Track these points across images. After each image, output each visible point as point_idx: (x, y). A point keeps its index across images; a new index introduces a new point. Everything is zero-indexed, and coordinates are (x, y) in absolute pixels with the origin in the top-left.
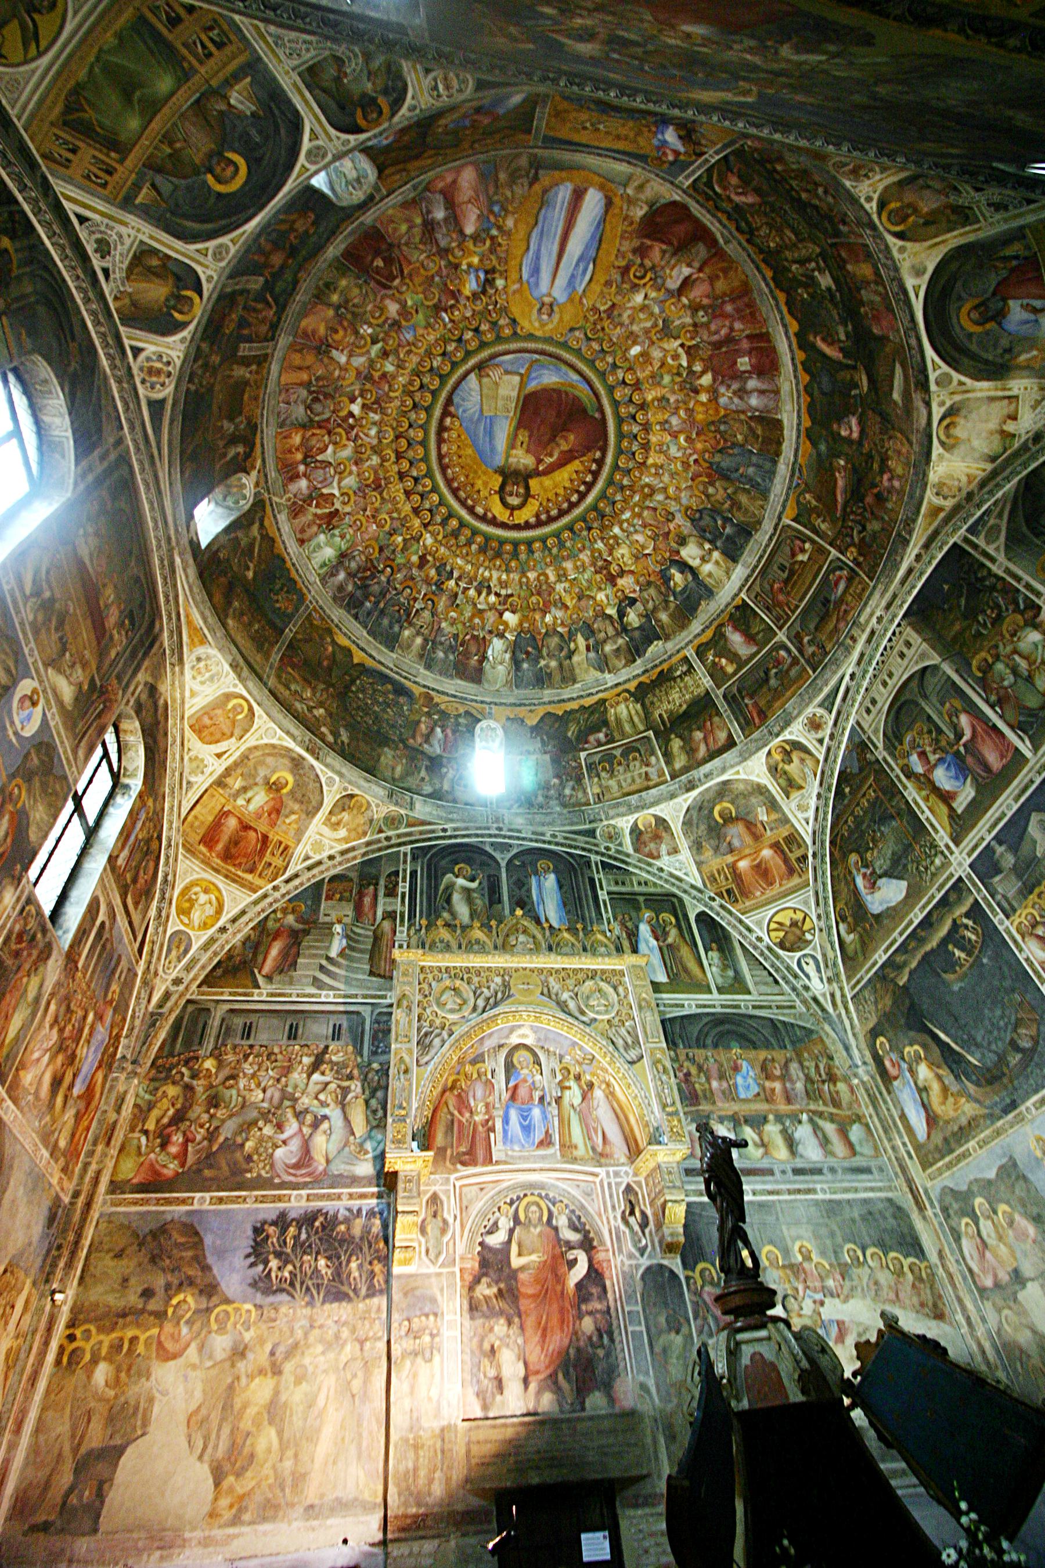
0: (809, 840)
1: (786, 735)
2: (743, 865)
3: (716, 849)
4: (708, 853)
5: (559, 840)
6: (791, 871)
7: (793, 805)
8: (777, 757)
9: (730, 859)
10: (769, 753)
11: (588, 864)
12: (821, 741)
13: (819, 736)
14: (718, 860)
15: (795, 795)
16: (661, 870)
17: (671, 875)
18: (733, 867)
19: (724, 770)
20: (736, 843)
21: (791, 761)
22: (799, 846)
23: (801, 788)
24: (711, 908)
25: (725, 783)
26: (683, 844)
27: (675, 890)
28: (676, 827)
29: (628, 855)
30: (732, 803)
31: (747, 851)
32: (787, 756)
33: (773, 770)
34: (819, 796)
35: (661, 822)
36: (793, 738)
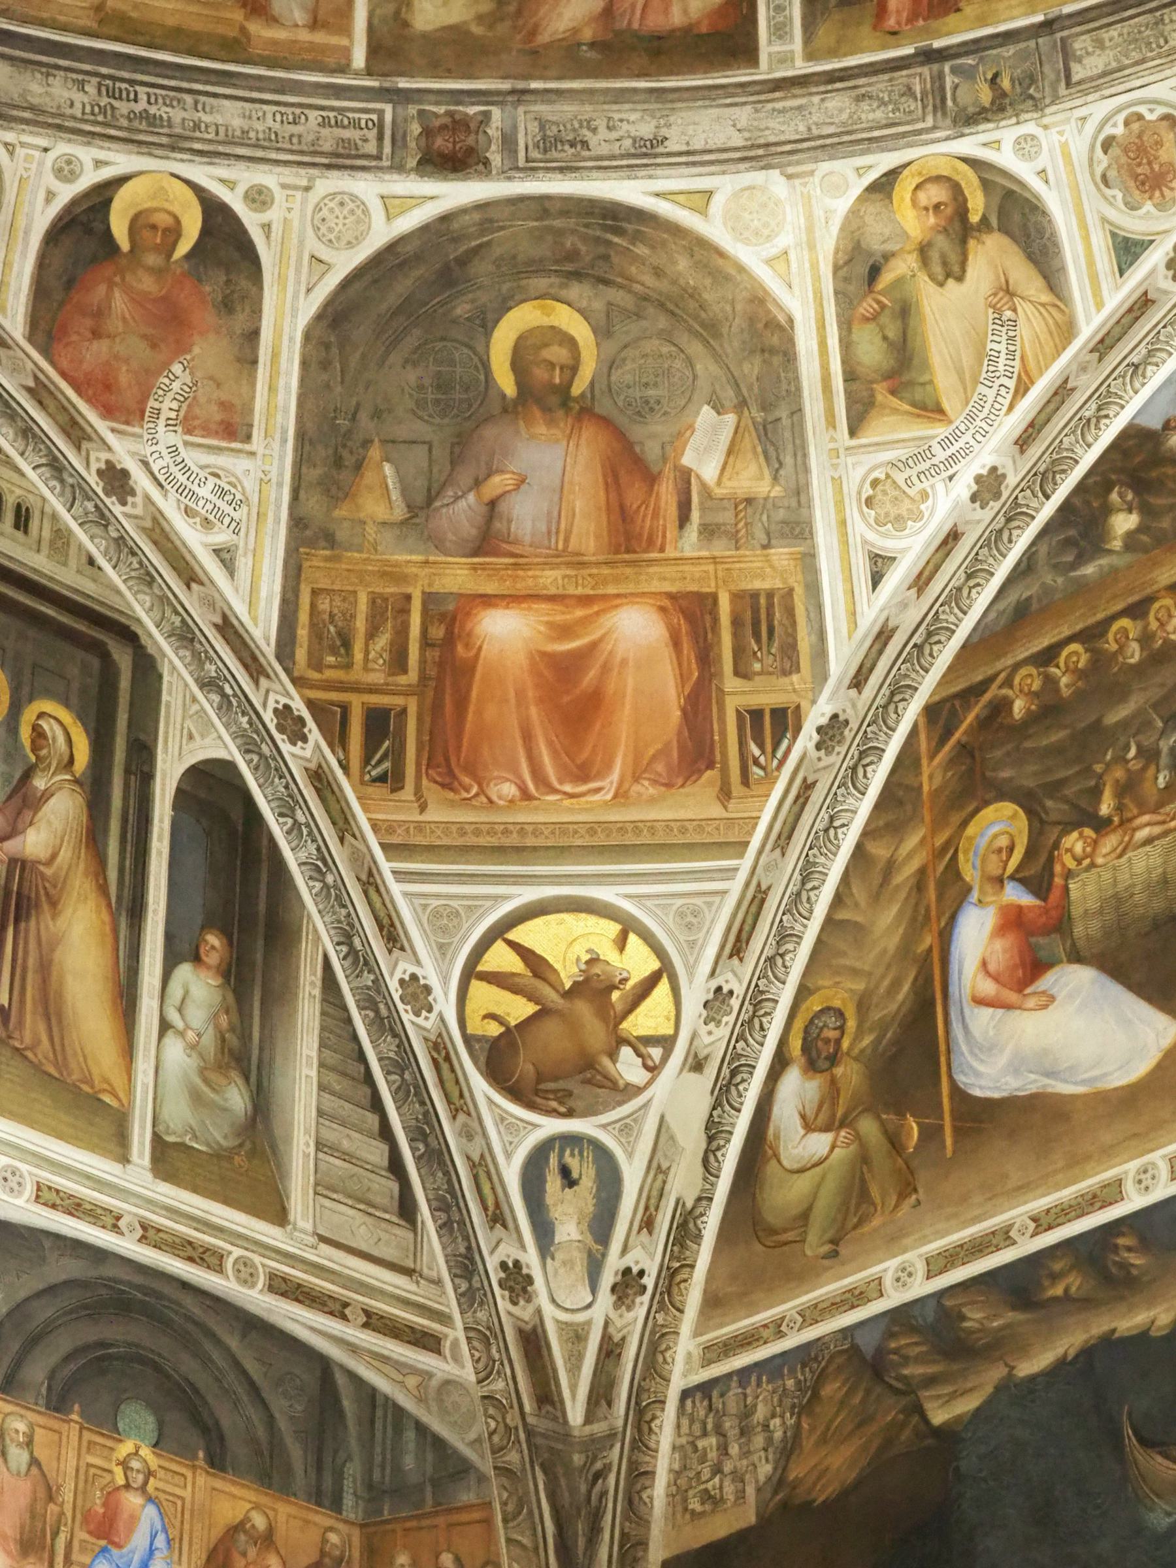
0: (841, 657)
1: (1003, 145)
6: (695, 754)
7: (858, 470)
8: (910, 219)
10: (884, 186)
12: (1128, 250)
13: (1134, 225)
15: (894, 433)
16: (117, 480)
18: (450, 619)
19: (646, 154)
21: (955, 271)
23: (933, 410)
25: (615, 216)
28: (288, 310)
30: (603, 332)
31: (550, 579)
32: (960, 228)
33: (861, 271)
34: (988, 486)
35: (226, 245)
36: (1024, 171)
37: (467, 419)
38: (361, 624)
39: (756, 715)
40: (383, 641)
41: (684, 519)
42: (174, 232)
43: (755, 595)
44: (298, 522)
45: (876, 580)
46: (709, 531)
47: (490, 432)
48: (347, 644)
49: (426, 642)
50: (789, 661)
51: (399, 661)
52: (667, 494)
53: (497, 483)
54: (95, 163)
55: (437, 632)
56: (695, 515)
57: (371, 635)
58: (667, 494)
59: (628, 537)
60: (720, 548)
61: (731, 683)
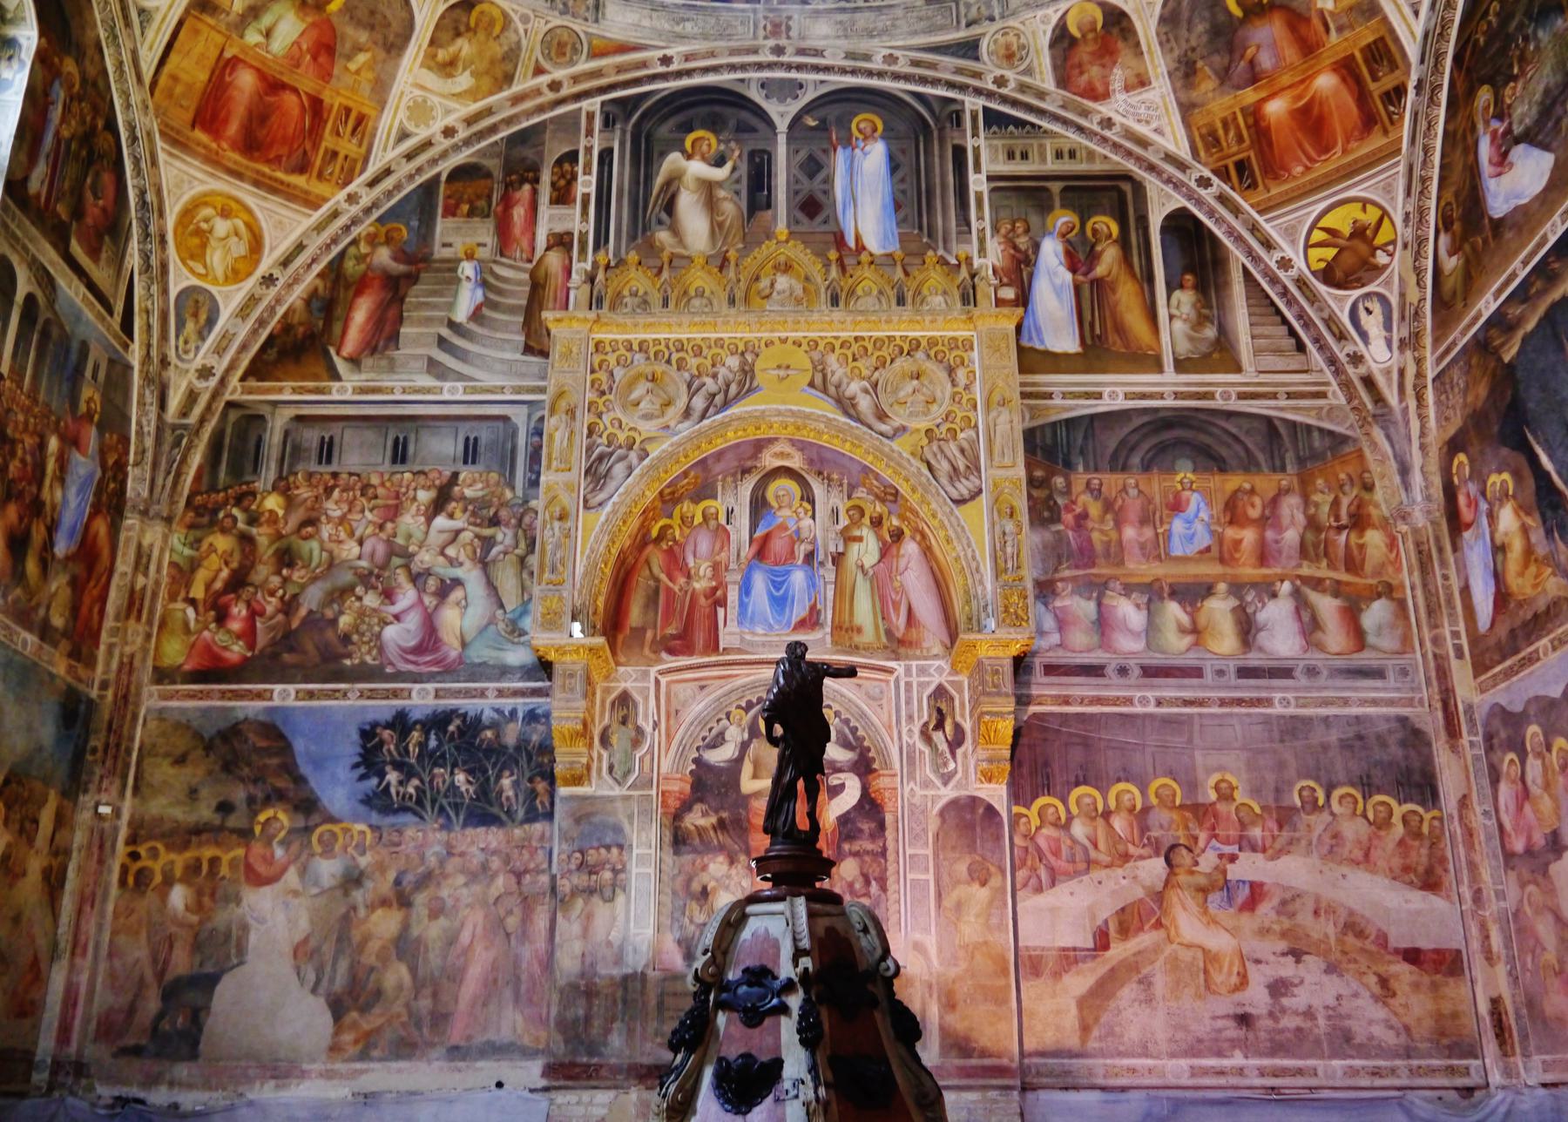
2: (1276, 108)
3: (1224, 76)
4: (1207, 85)
5: (902, 67)
6: (1369, 121)
9: (1250, 96)
11: (957, 118)
14: (1227, 100)
16: (1108, 123)
17: (1130, 135)
18: (1254, 114)
20: (1266, 61)
22: (1393, 66)
24: (1199, 202)
26: (1158, 64)
27: (1131, 166)
29: (1041, 95)
31: (1286, 80)
37: (1226, 36)
38: (1221, 132)
39: (1387, 94)
40: (1232, 134)
41: (1327, 30)
42: (1094, 22)
43: (1369, 46)
44: (1181, 105)
45: (1416, 13)
46: (1340, 29)
47: (1240, 33)
48: (1217, 141)
49: (1248, 127)
50: (1393, 66)
51: (1240, 139)
52: (1316, 22)
53: (1250, 52)
54: (1053, 15)
55: (1251, 121)
56: (1332, 26)
57: (1226, 133)
58: (1316, 22)
59: (1308, 48)
60: (1347, 34)
61: (1372, 86)
